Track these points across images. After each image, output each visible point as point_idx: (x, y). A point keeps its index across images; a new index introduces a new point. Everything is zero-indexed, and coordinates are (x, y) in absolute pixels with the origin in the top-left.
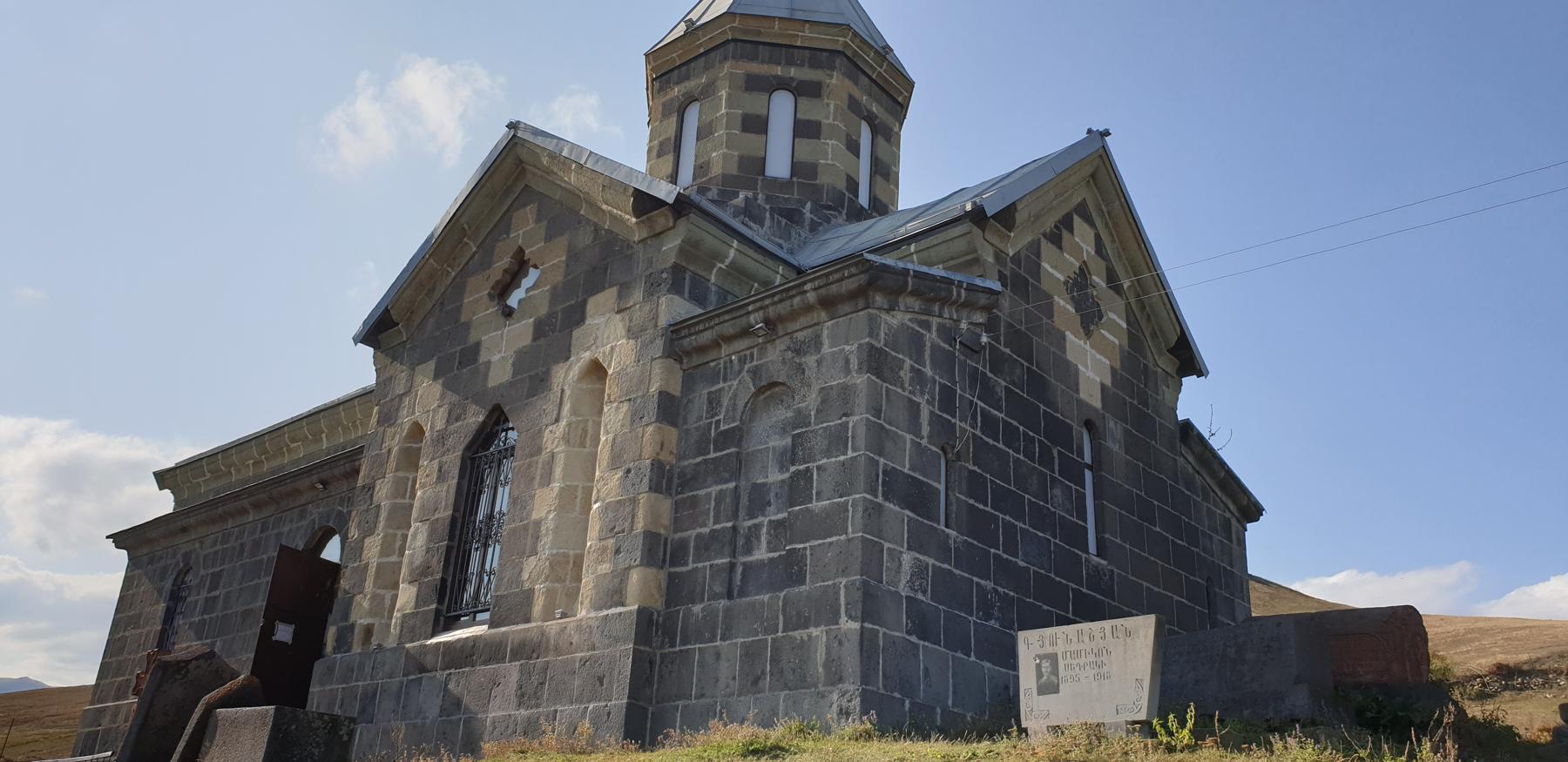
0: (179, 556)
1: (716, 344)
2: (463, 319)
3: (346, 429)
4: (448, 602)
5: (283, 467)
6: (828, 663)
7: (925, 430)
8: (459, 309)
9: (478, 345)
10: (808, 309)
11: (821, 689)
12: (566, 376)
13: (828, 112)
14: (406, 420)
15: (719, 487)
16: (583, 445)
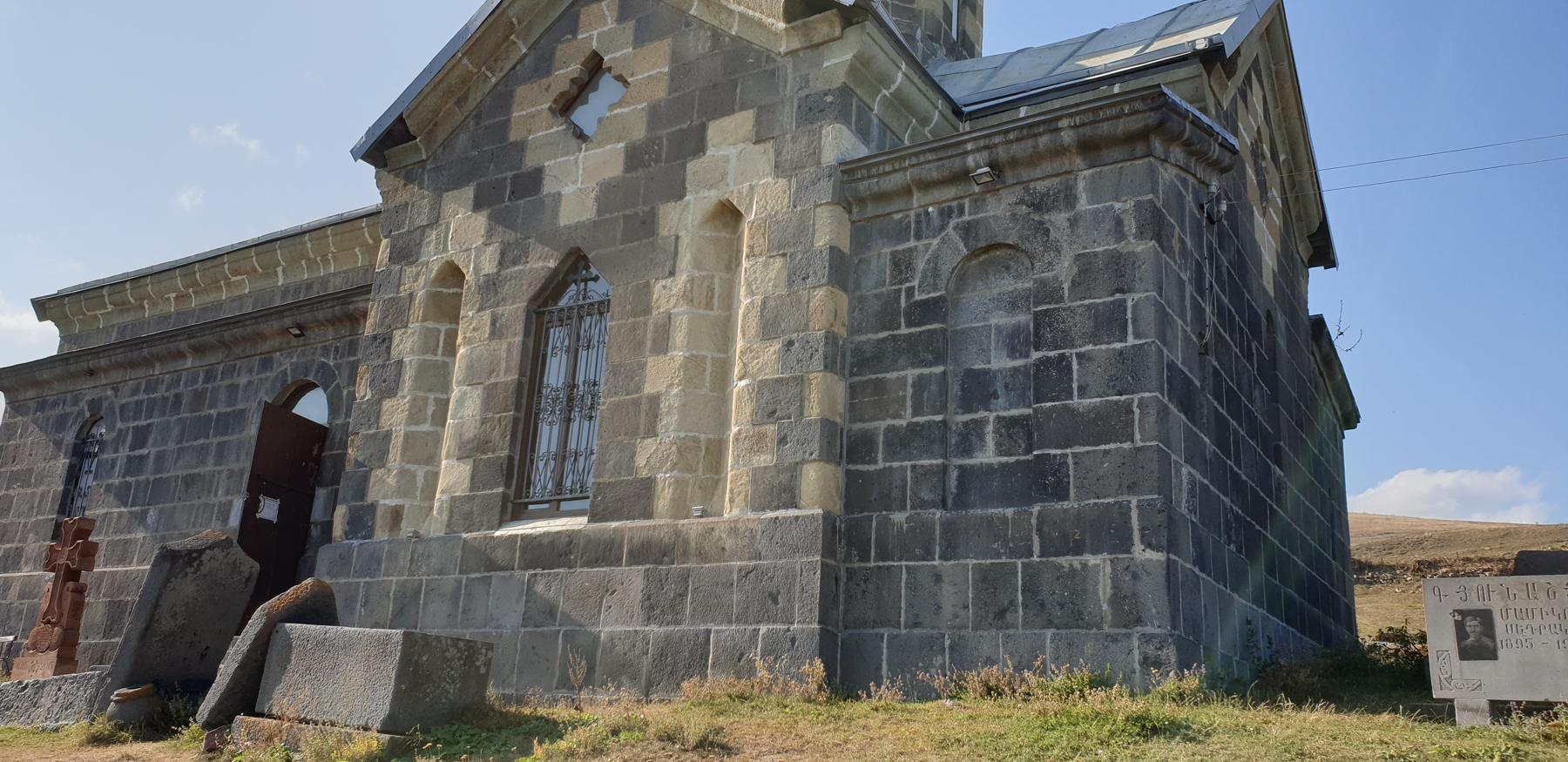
0: (83, 404)
1: (907, 192)
2: (513, 137)
3: (312, 264)
4: (513, 483)
5: (219, 305)
6: (1117, 600)
8: (505, 125)
9: (538, 173)
10: (1059, 151)
11: (1107, 629)
12: (683, 219)
14: (433, 259)
15: (918, 371)
16: (709, 306)
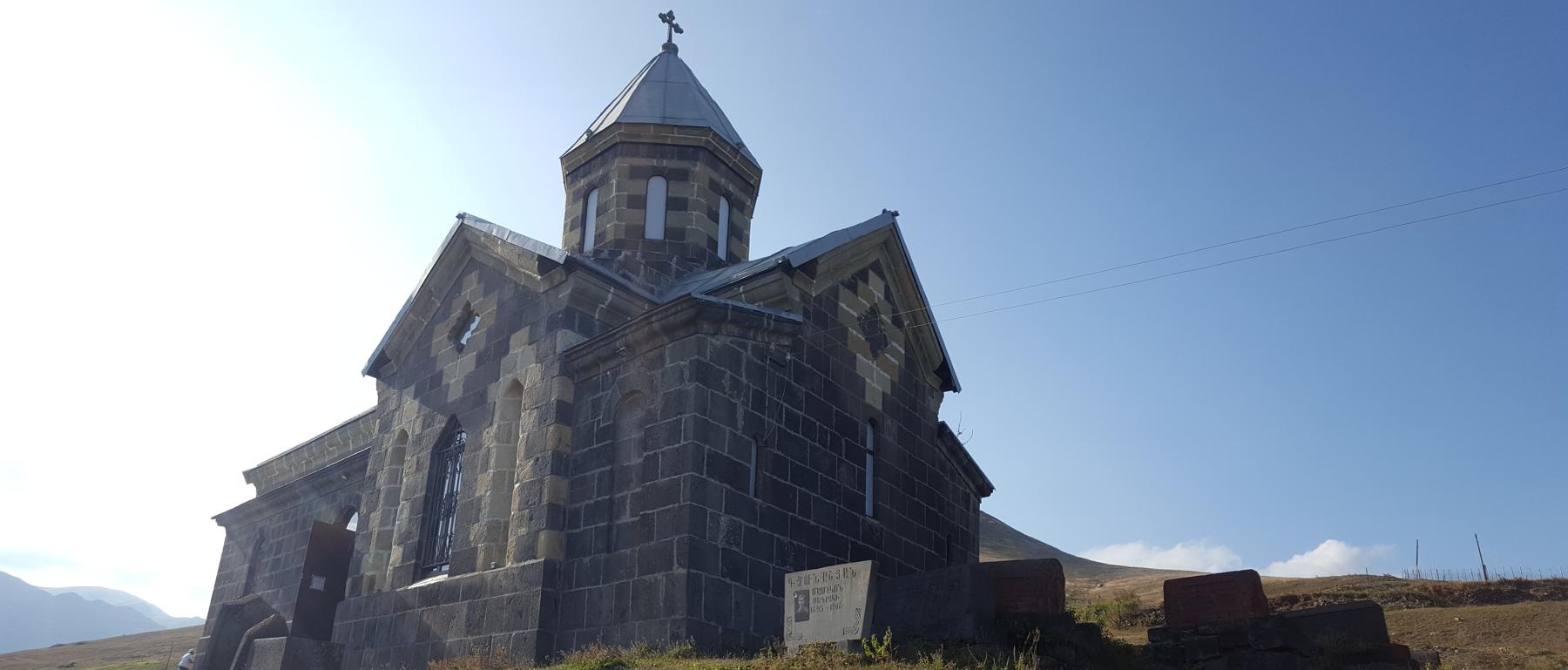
1: (596, 364)
7: (741, 423)
8: (429, 348)
9: (441, 372)
12: (497, 392)
13: (693, 191)
14: (396, 428)
16: (508, 441)
